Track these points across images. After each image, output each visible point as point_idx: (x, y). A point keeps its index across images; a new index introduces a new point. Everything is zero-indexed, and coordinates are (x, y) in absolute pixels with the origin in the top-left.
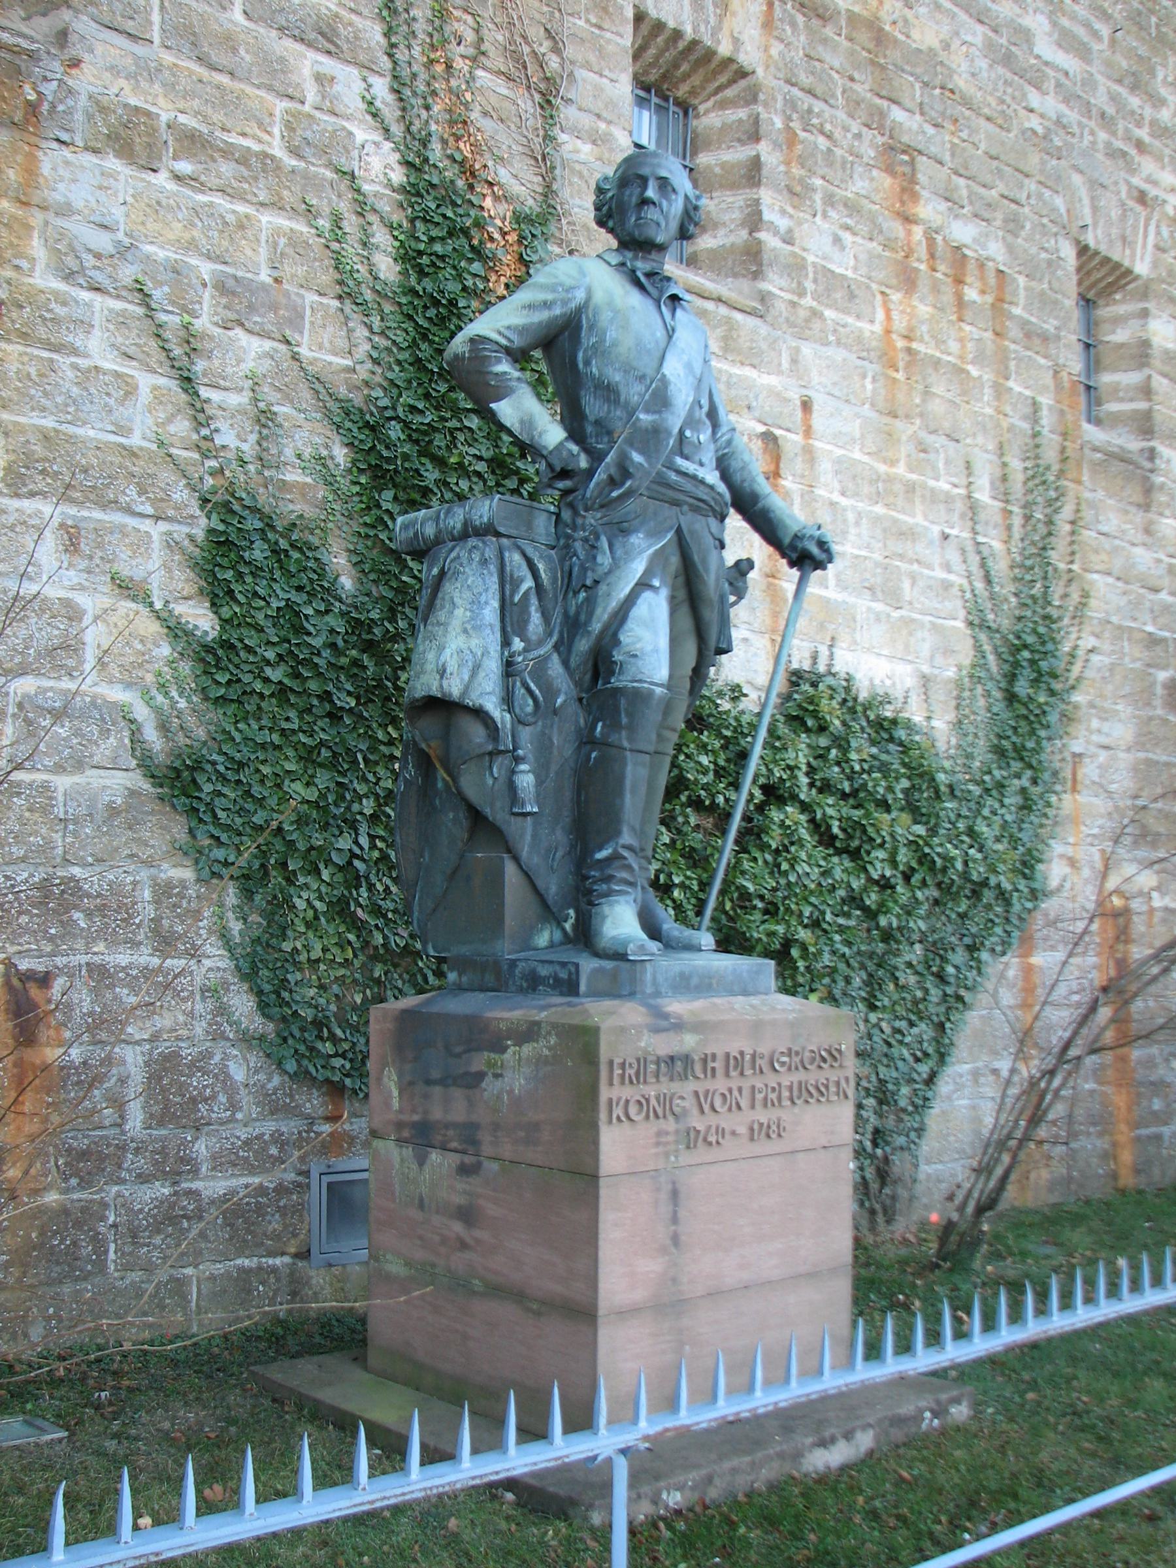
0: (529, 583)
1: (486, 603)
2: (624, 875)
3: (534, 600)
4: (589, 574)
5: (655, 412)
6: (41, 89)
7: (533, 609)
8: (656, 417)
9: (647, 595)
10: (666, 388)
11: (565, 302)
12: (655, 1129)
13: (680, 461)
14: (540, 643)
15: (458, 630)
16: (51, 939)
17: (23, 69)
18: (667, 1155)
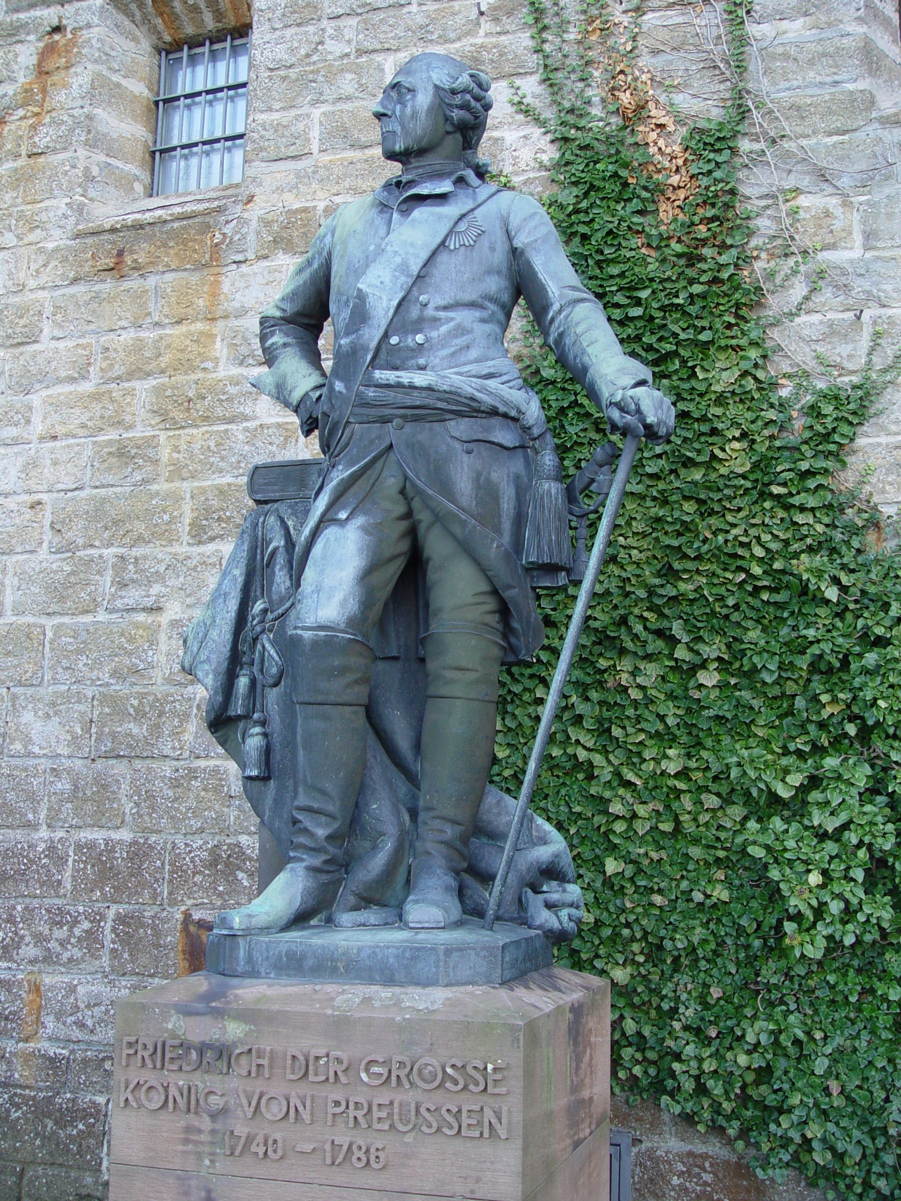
0: (278, 542)
3: (281, 559)
6: (225, 231)
8: (354, 336)
9: (330, 533)
11: (320, 254)
12: (183, 1123)
13: (380, 375)
16: (220, 895)
17: (212, 222)
18: (199, 1156)
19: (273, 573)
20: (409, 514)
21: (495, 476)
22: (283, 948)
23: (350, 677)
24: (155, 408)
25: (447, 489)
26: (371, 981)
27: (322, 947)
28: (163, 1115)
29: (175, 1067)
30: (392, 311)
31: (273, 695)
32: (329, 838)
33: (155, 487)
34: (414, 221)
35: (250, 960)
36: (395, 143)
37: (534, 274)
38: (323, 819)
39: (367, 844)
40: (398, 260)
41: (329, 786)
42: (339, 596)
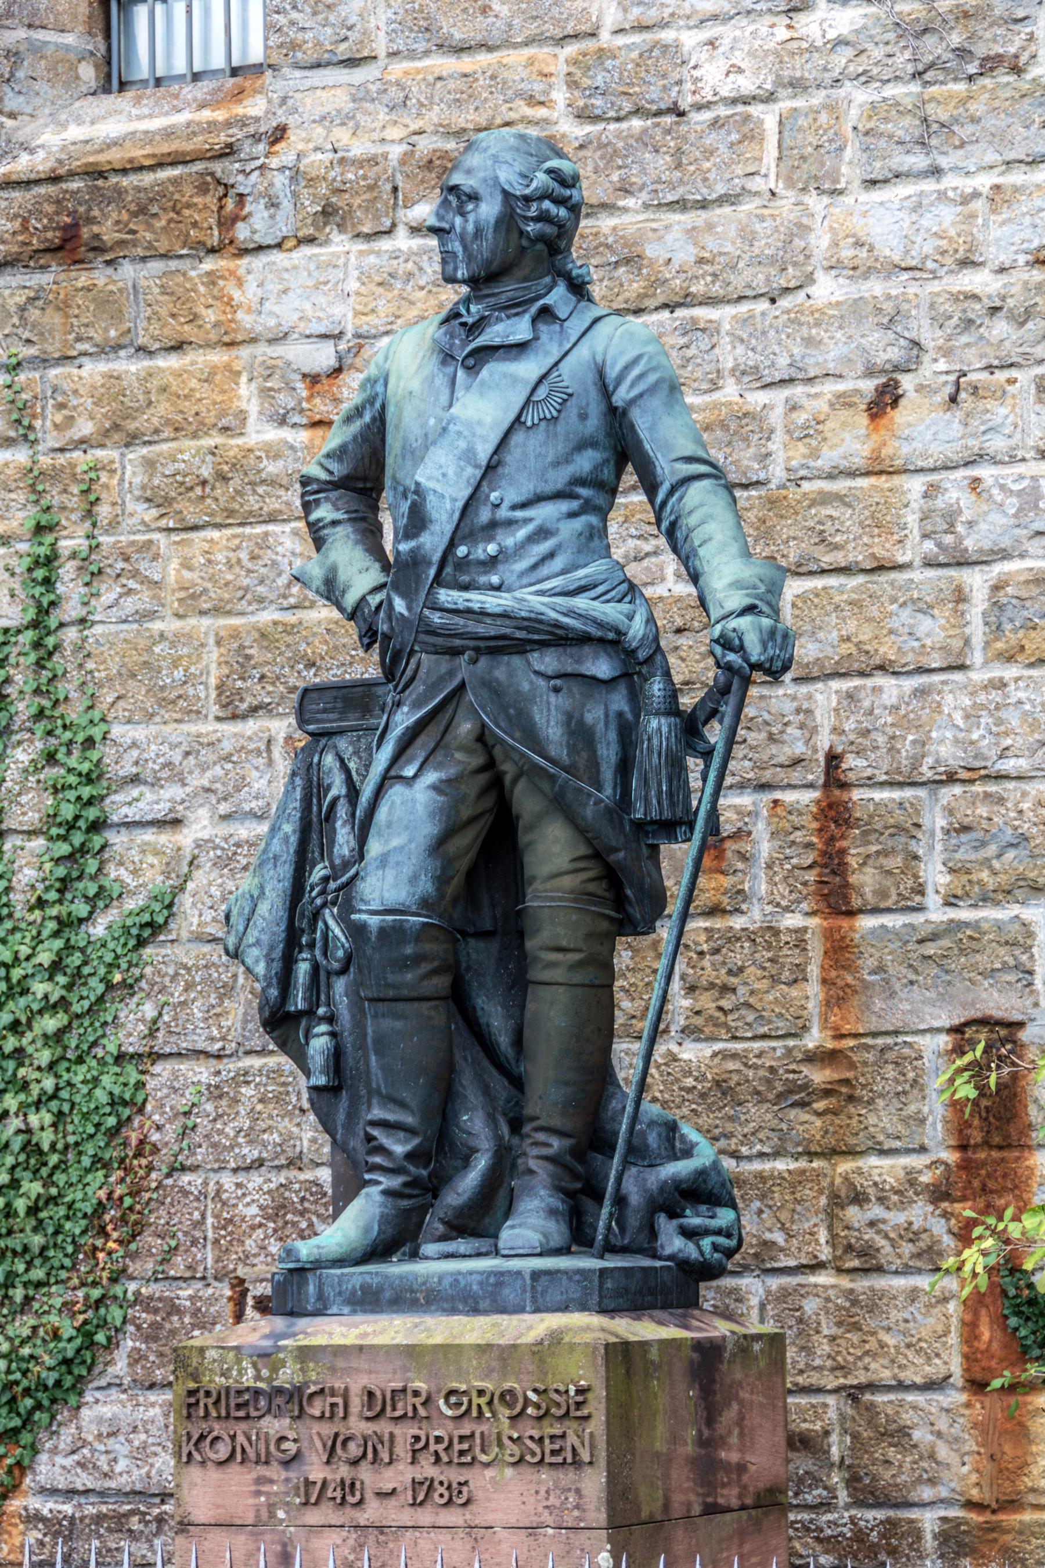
0: (338, 788)
7: (339, 824)
9: (396, 793)
12: (254, 1475)
20: (490, 765)
21: (589, 718)
23: (425, 967)
24: (149, 493)
25: (532, 737)
26: (453, 1311)
27: (401, 1277)
28: (234, 1468)
29: (241, 1413)
30: (457, 515)
31: (340, 985)
32: (409, 1156)
33: (157, 626)
34: (482, 384)
35: (321, 1296)
38: (401, 1135)
39: (459, 1163)
40: (462, 444)
41: (406, 1095)
42: (407, 870)
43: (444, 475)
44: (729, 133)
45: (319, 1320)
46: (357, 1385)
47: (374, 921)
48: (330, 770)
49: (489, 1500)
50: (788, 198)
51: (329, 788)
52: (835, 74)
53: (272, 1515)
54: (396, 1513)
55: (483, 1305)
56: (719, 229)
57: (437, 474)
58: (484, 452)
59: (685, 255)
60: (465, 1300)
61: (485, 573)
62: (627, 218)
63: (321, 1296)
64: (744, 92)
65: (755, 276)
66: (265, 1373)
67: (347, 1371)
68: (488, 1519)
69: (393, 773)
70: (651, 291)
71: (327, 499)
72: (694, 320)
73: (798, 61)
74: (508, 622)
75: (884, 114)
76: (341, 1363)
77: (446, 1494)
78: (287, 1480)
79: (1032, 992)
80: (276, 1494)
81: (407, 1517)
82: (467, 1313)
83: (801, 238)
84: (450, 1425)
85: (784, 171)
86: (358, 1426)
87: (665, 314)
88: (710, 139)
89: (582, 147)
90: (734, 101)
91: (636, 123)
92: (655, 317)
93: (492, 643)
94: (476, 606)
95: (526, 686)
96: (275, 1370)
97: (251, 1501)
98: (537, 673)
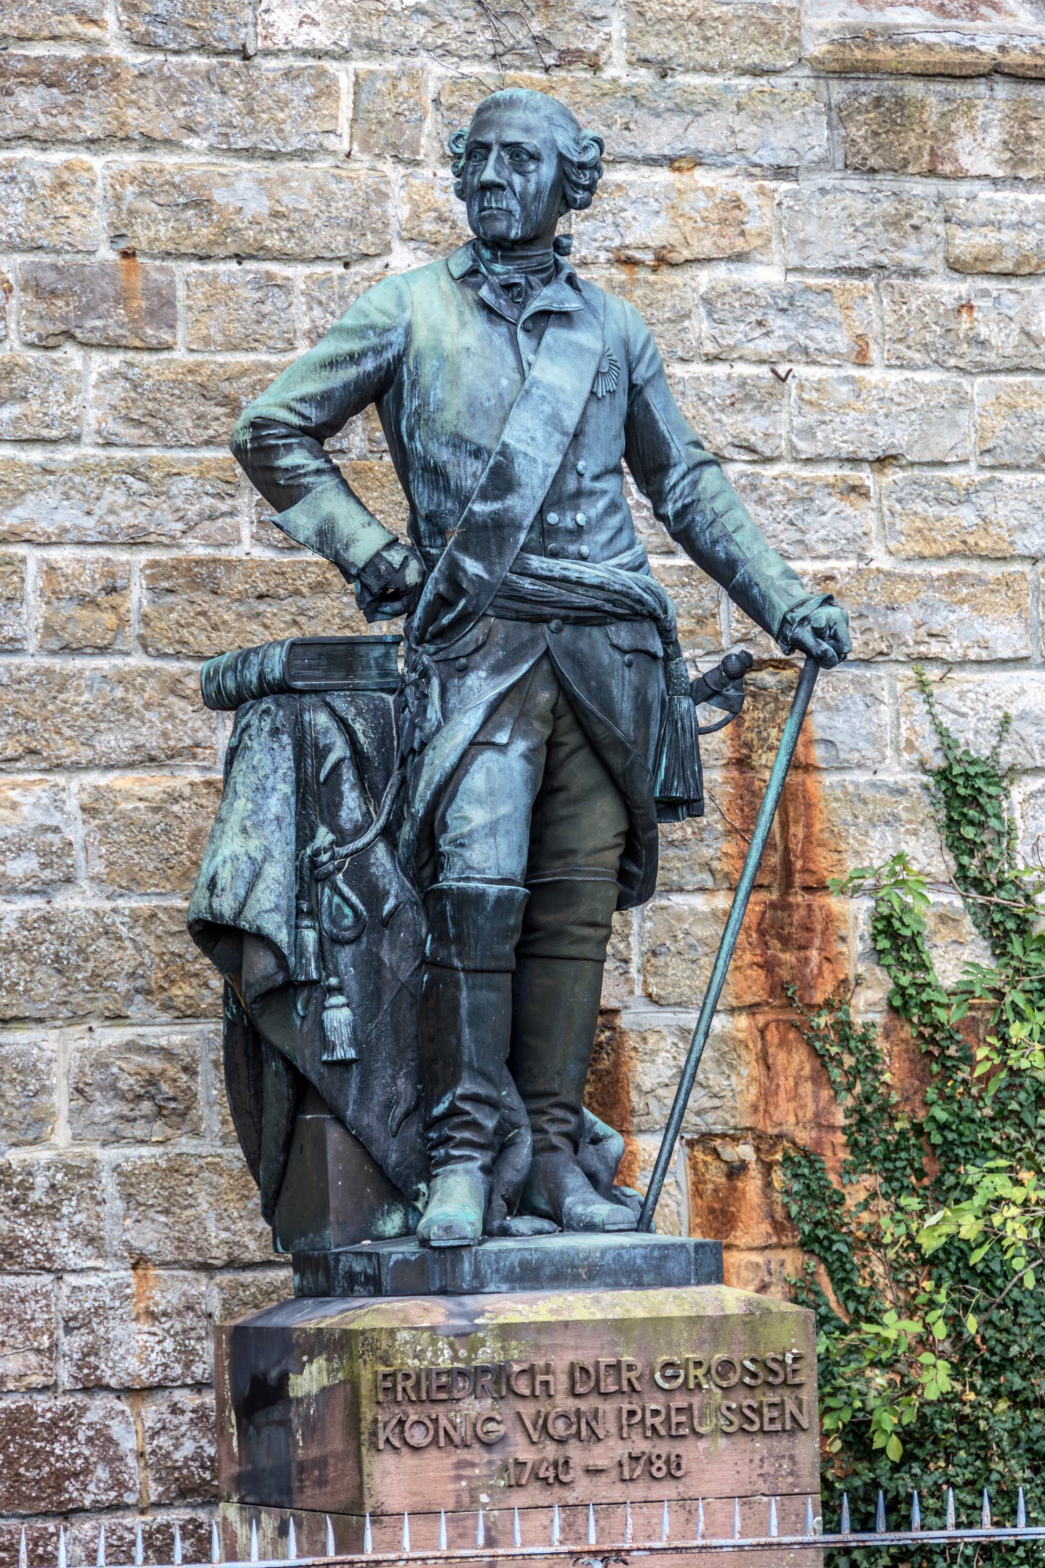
0: (339, 750)
1: (274, 789)
2: (467, 1135)
3: (348, 774)
4: (417, 734)
5: (495, 498)
7: (346, 787)
8: (497, 506)
9: (487, 758)
10: (512, 462)
11: (377, 351)
12: (453, 1459)
14: (359, 830)
15: (236, 829)
19: (341, 794)
22: (515, 1258)
26: (617, 1285)
27: (561, 1253)
28: (433, 1452)
29: (443, 1396)
30: (549, 481)
34: (549, 348)
35: (477, 1274)
36: (509, 227)
37: (652, 423)
38: (487, 1109)
40: (547, 409)
43: (533, 439)
44: (304, 86)
45: (481, 1298)
46: (561, 1362)
47: (493, 890)
48: (327, 730)
49: (702, 1471)
50: (363, 161)
51: (328, 749)
52: (414, 42)
53: (474, 1500)
54: (607, 1490)
55: (646, 1279)
56: (294, 184)
57: (526, 436)
58: (571, 420)
59: (258, 206)
60: (628, 1274)
61: (573, 542)
62: (187, 159)
63: (477, 1274)
64: (318, 45)
65: (334, 237)
66: (463, 1353)
67: (553, 1348)
68: (704, 1489)
69: (480, 739)
70: (221, 239)
71: (301, 445)
72: (269, 276)
73: (376, 23)
74: (600, 594)
75: (466, 91)
76: (545, 1341)
77: (664, 1468)
78: (490, 1462)
79: (628, 980)
80: (479, 1477)
81: (617, 1493)
82: (631, 1287)
83: (378, 205)
84: (661, 1397)
85: (358, 133)
86: (565, 1403)
87: (233, 266)
88: (283, 89)
89: (142, 75)
90: (305, 53)
91: (201, 61)
92: (223, 267)
93: (582, 614)
94: (573, 576)
95: (606, 660)
96: (473, 1349)
97: (451, 1486)
98: (613, 646)
